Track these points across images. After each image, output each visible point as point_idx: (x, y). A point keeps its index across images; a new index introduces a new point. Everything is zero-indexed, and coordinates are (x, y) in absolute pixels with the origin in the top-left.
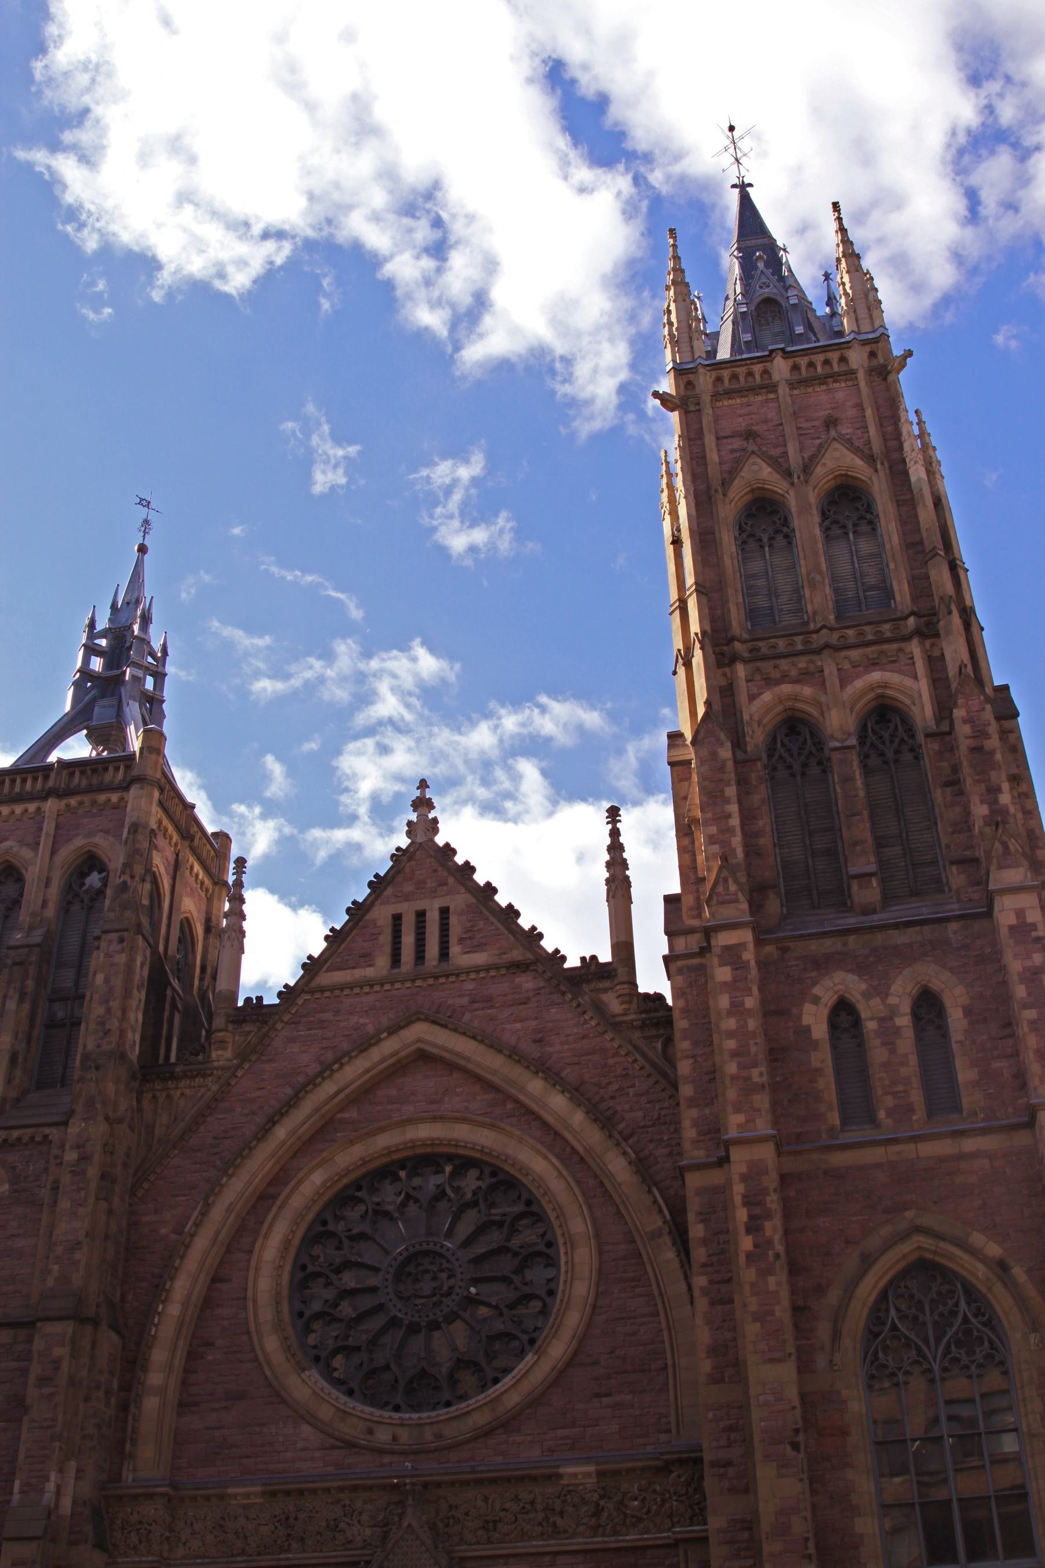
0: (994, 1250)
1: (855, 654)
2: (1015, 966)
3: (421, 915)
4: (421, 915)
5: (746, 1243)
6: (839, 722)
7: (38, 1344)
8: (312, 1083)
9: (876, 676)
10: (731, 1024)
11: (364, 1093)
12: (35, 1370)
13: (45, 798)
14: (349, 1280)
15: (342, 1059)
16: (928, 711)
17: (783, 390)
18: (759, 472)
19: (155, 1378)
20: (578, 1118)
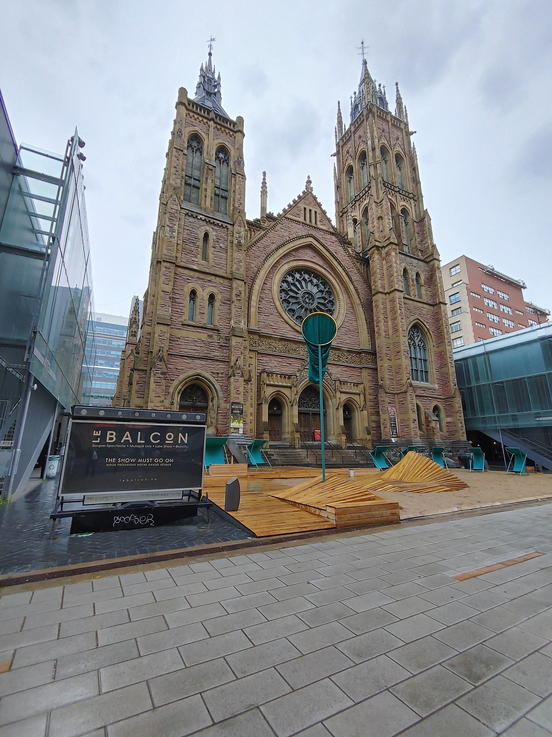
0: (428, 327)
1: (402, 196)
2: (437, 275)
3: (310, 210)
4: (310, 210)
5: (399, 311)
6: (399, 209)
7: (234, 285)
8: (289, 241)
9: (404, 203)
10: (395, 265)
11: (297, 249)
12: (234, 292)
13: (210, 120)
14: (291, 294)
15: (294, 239)
16: (414, 216)
17: (390, 124)
18: (384, 141)
19: (253, 303)
20: (344, 274)
